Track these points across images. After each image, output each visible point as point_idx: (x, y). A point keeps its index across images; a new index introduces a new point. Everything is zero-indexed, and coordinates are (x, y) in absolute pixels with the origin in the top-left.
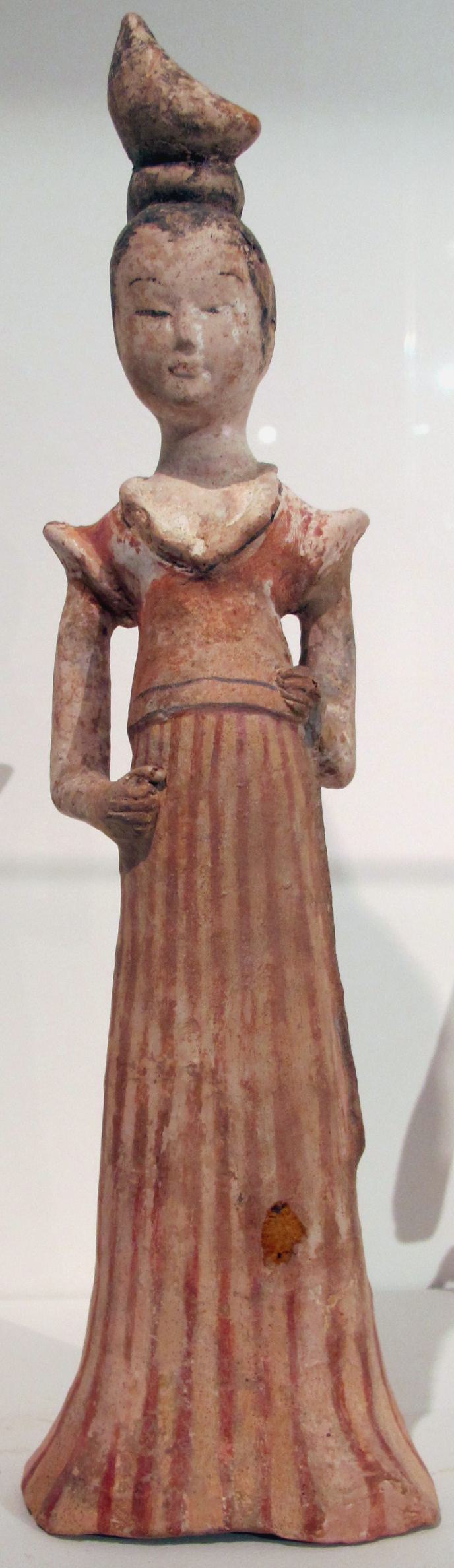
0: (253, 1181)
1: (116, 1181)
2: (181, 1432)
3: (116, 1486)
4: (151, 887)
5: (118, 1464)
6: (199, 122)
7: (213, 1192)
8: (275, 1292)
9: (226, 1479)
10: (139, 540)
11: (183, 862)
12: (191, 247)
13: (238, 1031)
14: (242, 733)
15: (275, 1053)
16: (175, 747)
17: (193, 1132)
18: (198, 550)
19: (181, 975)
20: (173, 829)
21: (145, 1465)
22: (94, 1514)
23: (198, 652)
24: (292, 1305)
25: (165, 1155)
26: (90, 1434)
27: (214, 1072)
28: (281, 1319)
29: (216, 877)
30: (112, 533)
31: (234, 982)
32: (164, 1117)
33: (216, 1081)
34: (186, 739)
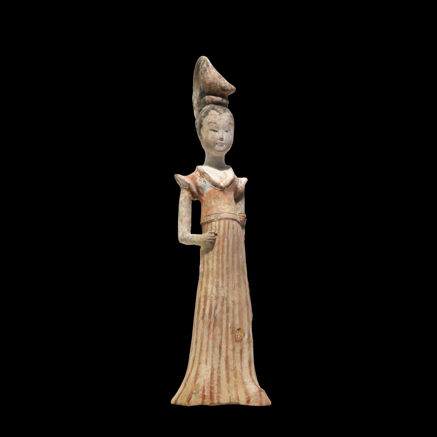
0: (233, 324)
1: (204, 323)
2: (219, 381)
3: (206, 393)
4: (213, 257)
5: (206, 388)
6: (226, 88)
7: (225, 325)
8: (238, 349)
9: (229, 391)
10: (206, 180)
11: (221, 252)
12: (223, 117)
13: (231, 289)
14: (233, 225)
15: (239, 295)
16: (219, 227)
17: (222, 311)
18: (222, 184)
19: (220, 276)
20: (219, 244)
21: (212, 388)
22: (201, 400)
23: (223, 207)
24: (241, 352)
25: (216, 316)
26: (197, 383)
27: (227, 298)
28: (239, 355)
29: (228, 255)
30: (197, 178)
31: (231, 278)
32: (216, 308)
33: (227, 300)
34: (222, 225)
